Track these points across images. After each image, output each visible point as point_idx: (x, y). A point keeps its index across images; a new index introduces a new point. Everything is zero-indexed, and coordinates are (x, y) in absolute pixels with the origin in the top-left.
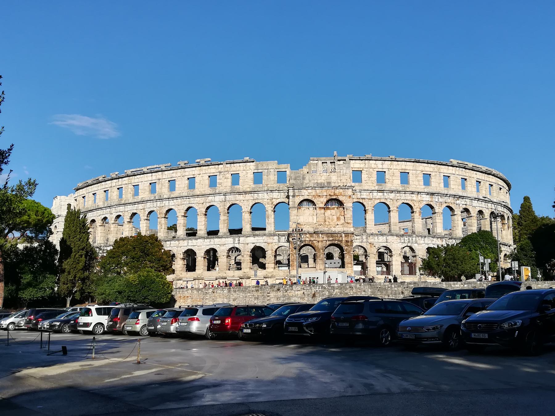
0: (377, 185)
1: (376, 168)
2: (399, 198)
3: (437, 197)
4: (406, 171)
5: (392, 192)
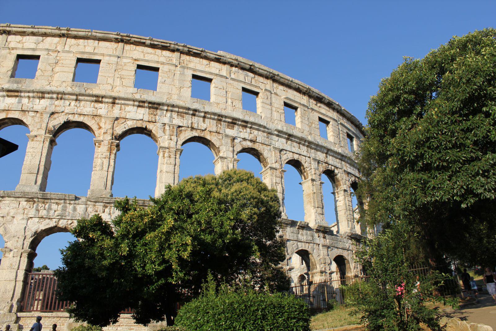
0: (9, 82)
1: (16, 48)
2: (58, 109)
3: (169, 114)
4: (93, 56)
5: (42, 94)
